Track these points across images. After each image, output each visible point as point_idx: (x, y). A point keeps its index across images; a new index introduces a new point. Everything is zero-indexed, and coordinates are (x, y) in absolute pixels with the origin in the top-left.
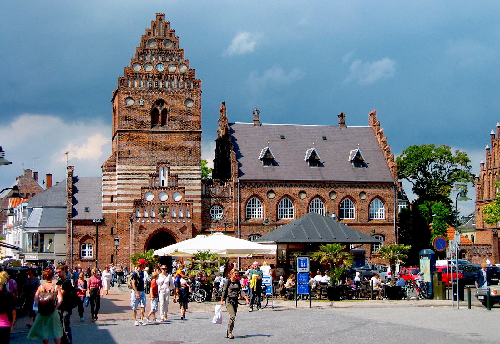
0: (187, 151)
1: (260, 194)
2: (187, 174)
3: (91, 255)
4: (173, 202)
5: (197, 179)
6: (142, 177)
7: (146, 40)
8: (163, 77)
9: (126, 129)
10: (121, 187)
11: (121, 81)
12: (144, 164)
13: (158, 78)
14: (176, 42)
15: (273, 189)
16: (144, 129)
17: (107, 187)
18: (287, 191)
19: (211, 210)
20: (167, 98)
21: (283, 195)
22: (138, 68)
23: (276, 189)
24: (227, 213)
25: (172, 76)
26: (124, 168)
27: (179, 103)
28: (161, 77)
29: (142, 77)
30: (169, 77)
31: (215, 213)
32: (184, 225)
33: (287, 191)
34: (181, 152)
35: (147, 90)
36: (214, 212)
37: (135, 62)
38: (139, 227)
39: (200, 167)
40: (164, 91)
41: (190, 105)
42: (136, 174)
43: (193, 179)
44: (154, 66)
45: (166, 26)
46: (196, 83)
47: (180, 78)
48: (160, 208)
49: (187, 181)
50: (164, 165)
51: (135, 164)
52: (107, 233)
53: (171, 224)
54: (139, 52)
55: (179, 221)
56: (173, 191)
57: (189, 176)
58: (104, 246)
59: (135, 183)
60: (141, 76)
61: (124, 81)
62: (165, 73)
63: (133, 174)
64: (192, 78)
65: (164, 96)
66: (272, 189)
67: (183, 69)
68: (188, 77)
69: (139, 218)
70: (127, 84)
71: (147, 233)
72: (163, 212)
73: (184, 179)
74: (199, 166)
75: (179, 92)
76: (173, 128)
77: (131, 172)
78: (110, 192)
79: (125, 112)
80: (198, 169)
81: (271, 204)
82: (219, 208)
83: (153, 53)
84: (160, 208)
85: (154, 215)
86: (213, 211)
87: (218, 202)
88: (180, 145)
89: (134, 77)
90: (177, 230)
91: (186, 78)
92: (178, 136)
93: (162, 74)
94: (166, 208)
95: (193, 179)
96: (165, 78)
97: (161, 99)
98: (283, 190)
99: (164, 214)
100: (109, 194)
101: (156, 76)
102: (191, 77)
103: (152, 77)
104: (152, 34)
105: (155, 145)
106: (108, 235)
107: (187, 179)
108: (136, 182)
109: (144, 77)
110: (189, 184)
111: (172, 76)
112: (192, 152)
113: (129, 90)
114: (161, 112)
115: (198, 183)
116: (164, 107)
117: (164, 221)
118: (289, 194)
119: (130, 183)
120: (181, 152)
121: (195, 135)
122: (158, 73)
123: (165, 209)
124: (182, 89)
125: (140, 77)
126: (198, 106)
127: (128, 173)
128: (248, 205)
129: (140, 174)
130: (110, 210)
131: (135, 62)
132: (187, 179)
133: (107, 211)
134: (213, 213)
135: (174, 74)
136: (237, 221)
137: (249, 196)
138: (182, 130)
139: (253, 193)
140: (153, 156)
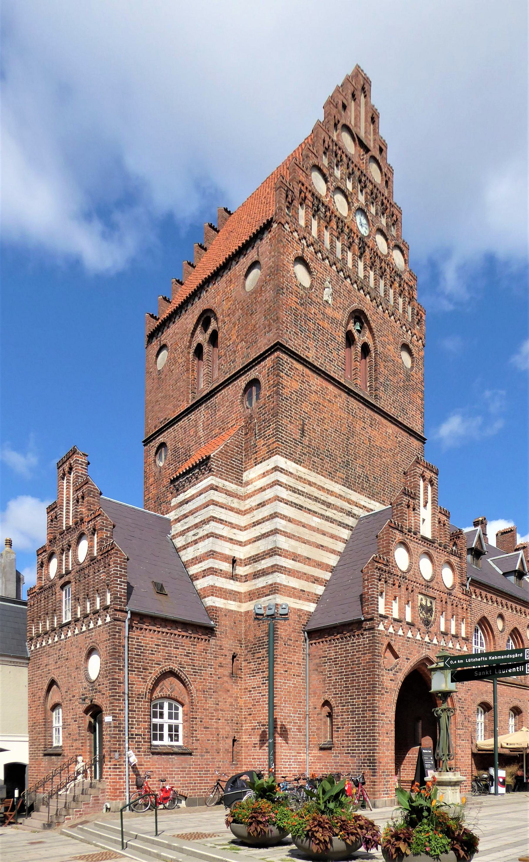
6: (328, 514)
10: (285, 527)
12: (331, 476)
17: (222, 526)
26: (291, 471)
42: (316, 499)
51: (313, 468)
52: (221, 670)
58: (216, 710)
59: (313, 525)
63: (309, 497)
77: (307, 489)
78: (228, 545)
100: (227, 552)
106: (224, 676)
108: (315, 521)
119: (303, 520)
127: (300, 488)
129: (324, 503)
130: (229, 602)
133: (223, 601)
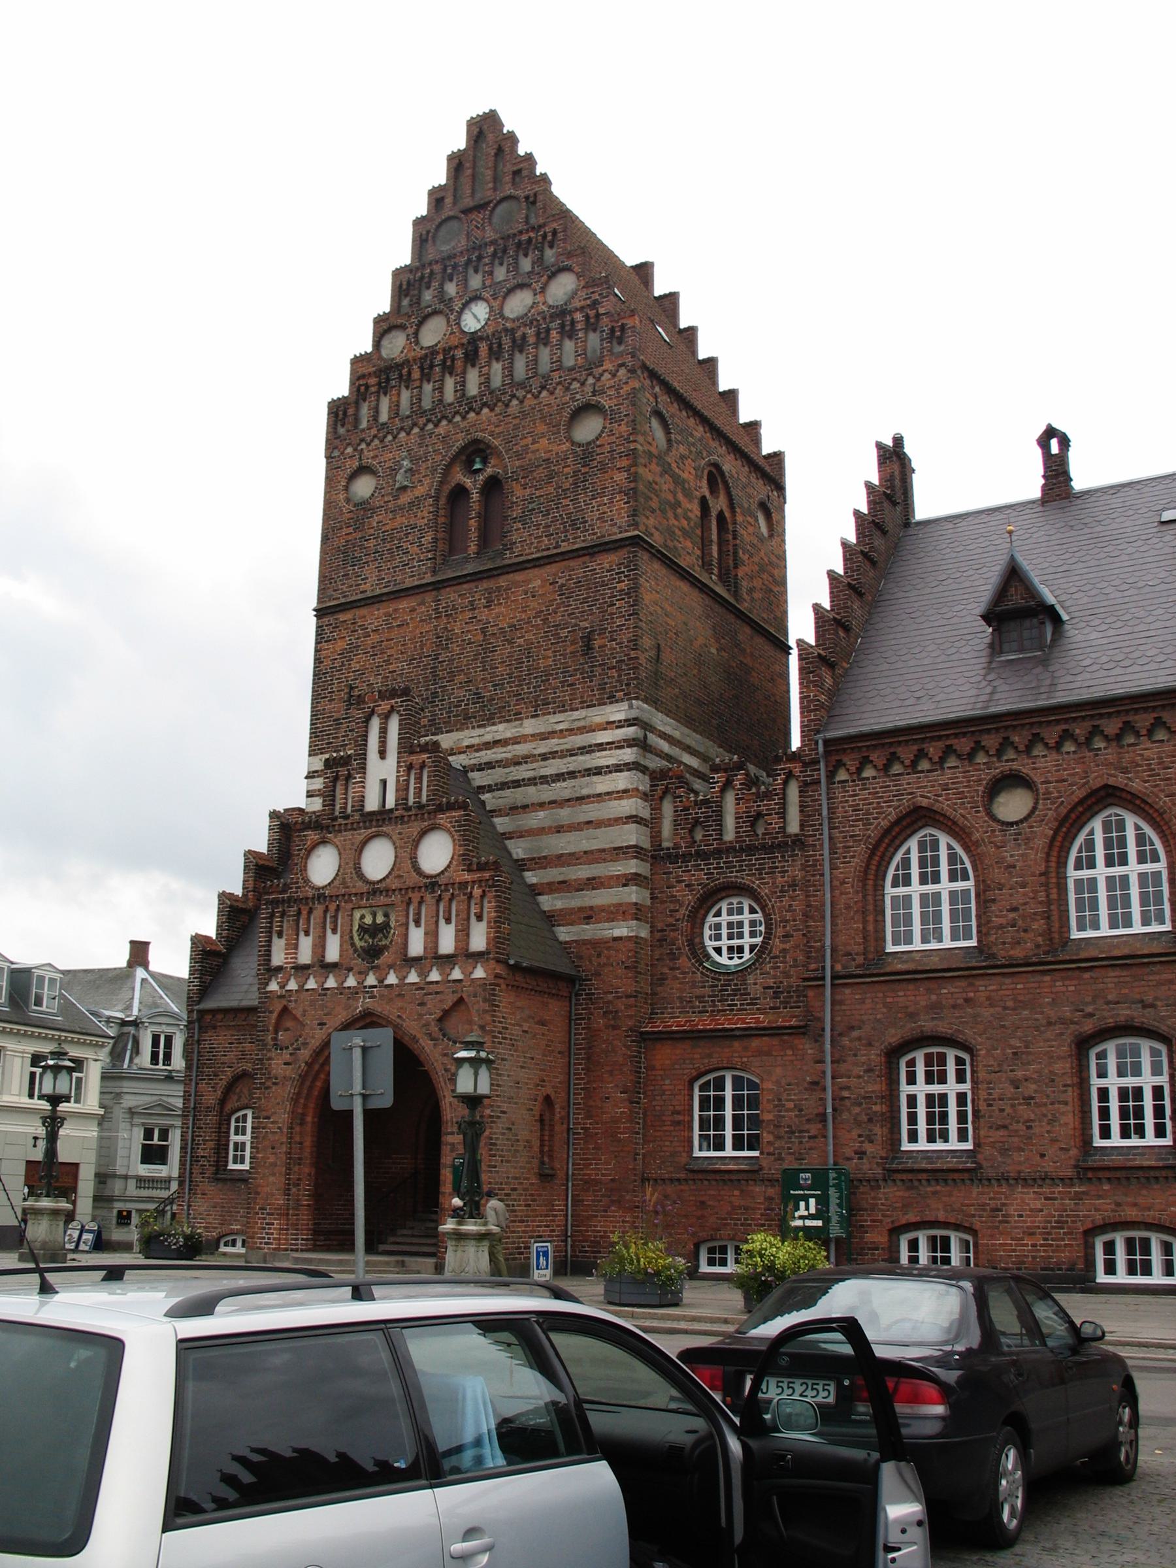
0: (573, 643)
1: (944, 806)
2: (572, 753)
3: (242, 1162)
4: (414, 879)
5: (618, 768)
7: (428, 232)
8: (483, 348)
9: (343, 600)
11: (337, 415)
13: (466, 355)
14: (535, 195)
15: (1023, 766)
16: (409, 583)
18: (1108, 764)
19: (711, 920)
20: (497, 430)
21: (1081, 793)
22: (396, 345)
23: (1043, 765)
24: (780, 932)
25: (519, 334)
27: (543, 436)
28: (476, 351)
29: (409, 373)
30: (506, 341)
31: (730, 937)
32: (456, 997)
33: (1108, 764)
34: (550, 653)
35: (422, 421)
36: (724, 932)
37: (384, 327)
38: (275, 1015)
39: (631, 707)
40: (485, 405)
41: (588, 429)
43: (598, 771)
44: (452, 317)
45: (500, 151)
46: (612, 330)
47: (548, 330)
48: (363, 917)
49: (569, 783)
50: (385, 706)
53: (400, 991)
54: (401, 285)
55: (435, 976)
56: (415, 828)
57: (581, 758)
60: (405, 371)
61: (345, 413)
62: (490, 331)
64: (598, 315)
65: (484, 424)
66: (1015, 766)
67: (562, 288)
68: (578, 316)
69: (279, 969)
70: (357, 420)
71: (305, 1044)
72: (373, 936)
73: (559, 777)
74: (625, 705)
75: (543, 387)
76: (517, 549)
79: (345, 531)
80: (621, 716)
81: (1012, 854)
82: (746, 909)
83: (449, 271)
84: (363, 917)
85: (333, 953)
86: (718, 926)
87: (734, 876)
88: (545, 620)
89: (379, 384)
90: (427, 1025)
91: (573, 323)
92: (536, 579)
93: (481, 339)
94: (386, 915)
95: (598, 771)
96: (490, 349)
97: (476, 441)
98: (1081, 761)
99: (373, 947)
101: (459, 353)
102: (592, 313)
103: (444, 361)
104: (449, 201)
105: (443, 640)
107: (572, 774)
109: (416, 375)
110: (581, 799)
111: (519, 334)
112: (596, 643)
113: (362, 440)
114: (475, 496)
115: (621, 787)
116: (489, 471)
117: (371, 980)
118: (1119, 780)
120: (550, 653)
121: (608, 560)
122: (465, 341)
123: (380, 919)
124: (556, 375)
125: (401, 376)
126: (624, 428)
128: (896, 877)
131: (385, 326)
132: (572, 774)
134: (718, 937)
135: (525, 320)
136: (823, 968)
137: (885, 824)
138: (559, 551)
139: (906, 803)
140: (435, 694)
